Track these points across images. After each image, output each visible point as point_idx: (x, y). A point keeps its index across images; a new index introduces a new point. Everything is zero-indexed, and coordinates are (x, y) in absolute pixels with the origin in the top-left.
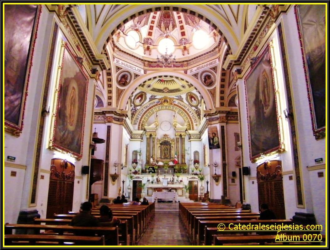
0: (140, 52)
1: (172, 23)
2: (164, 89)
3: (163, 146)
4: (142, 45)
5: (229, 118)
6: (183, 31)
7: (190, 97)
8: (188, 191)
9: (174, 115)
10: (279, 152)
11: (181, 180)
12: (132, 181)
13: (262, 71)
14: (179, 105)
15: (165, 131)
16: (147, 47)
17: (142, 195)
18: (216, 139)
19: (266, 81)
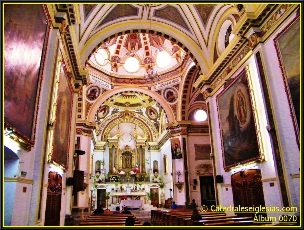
0: (108, 69)
1: (138, 43)
2: (126, 103)
3: (125, 157)
4: (110, 62)
5: (190, 131)
6: (147, 51)
8: (150, 198)
9: (135, 127)
10: (258, 162)
11: (143, 188)
12: (96, 190)
13: (237, 90)
14: (139, 118)
15: (126, 142)
16: (114, 64)
18: (178, 150)
19: (242, 100)
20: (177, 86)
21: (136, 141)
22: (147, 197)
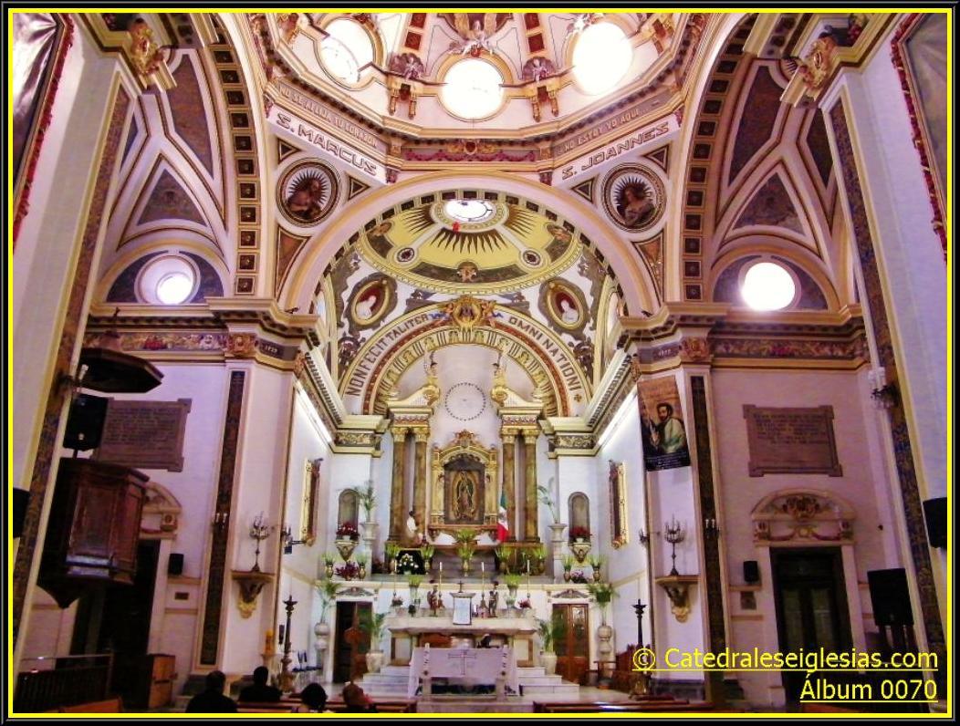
0: (375, 101)
2: (460, 269)
3: (456, 476)
4: (382, 78)
5: (721, 349)
6: (534, 32)
7: (555, 296)
8: (551, 644)
11: (525, 599)
12: (333, 603)
14: (515, 327)
15: (461, 420)
17: (369, 661)
18: (672, 428)
20: (661, 155)
21: (502, 415)
22: (539, 640)
